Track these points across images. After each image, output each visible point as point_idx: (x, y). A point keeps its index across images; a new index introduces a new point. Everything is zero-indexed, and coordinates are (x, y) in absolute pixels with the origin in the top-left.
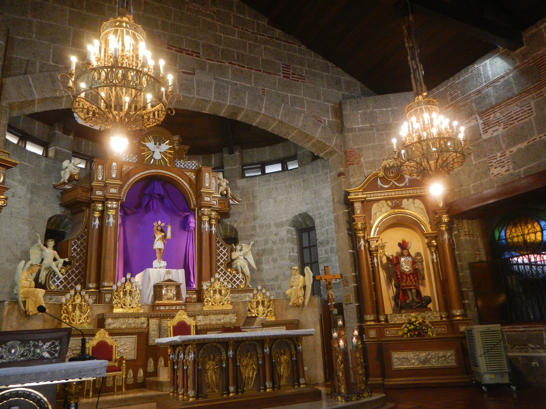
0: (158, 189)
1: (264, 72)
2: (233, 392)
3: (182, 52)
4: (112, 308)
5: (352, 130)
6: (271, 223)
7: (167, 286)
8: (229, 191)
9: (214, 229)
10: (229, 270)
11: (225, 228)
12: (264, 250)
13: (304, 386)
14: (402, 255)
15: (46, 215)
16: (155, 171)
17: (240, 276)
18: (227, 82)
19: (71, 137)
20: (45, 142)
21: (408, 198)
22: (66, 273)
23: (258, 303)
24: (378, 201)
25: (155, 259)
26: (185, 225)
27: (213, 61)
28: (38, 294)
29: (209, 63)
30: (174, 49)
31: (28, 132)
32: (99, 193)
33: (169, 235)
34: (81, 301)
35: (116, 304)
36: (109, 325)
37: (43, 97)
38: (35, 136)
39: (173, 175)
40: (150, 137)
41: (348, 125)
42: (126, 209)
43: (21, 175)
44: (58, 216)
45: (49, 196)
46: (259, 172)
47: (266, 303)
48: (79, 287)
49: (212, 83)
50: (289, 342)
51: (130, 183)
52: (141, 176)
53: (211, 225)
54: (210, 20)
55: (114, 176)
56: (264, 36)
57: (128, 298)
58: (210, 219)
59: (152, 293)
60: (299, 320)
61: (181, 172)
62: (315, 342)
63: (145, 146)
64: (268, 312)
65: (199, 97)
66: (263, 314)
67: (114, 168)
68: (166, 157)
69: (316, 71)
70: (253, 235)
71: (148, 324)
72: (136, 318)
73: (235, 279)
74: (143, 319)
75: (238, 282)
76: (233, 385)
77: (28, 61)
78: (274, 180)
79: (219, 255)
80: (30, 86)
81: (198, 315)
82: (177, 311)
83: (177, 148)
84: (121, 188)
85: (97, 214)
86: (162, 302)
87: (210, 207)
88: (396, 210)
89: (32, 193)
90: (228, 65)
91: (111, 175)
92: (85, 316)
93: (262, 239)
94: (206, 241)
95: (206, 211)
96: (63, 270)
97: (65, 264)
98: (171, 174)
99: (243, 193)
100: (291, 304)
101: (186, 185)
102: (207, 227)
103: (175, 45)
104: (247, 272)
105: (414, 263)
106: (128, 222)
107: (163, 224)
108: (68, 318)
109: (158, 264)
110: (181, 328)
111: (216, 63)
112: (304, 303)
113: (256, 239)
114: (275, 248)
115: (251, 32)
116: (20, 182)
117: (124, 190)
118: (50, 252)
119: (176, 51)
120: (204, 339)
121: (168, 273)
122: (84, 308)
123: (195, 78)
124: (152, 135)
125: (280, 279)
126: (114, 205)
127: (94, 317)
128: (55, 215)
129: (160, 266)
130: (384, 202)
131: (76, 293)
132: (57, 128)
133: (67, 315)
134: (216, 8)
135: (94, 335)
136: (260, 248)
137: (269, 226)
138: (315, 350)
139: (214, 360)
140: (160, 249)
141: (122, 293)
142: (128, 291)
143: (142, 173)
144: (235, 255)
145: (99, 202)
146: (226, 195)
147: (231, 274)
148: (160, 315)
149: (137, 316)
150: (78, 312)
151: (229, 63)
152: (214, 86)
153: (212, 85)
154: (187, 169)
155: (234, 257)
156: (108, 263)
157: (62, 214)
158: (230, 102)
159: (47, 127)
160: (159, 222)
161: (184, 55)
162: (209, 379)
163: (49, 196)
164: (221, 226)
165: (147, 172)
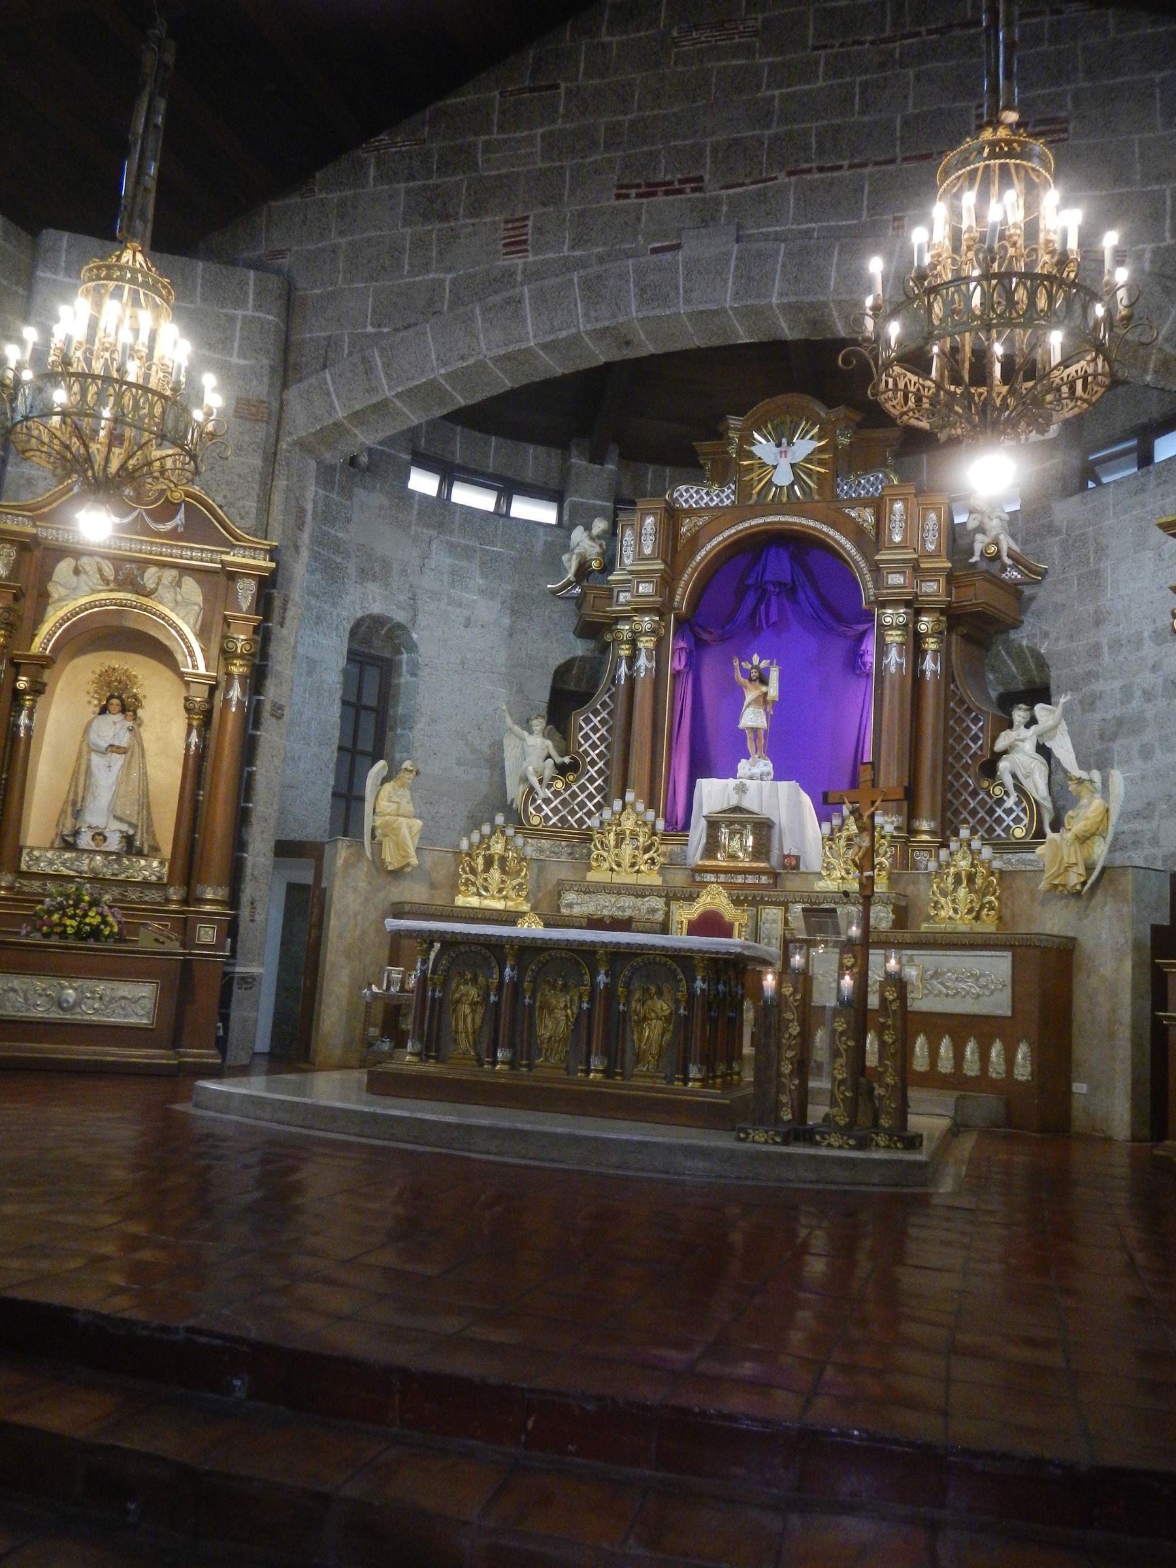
1: (905, 159)
2: (503, 1063)
3: (654, 194)
6: (1142, 632)
7: (730, 823)
10: (986, 784)
11: (1018, 654)
12: (1120, 722)
13: (698, 1084)
15: (550, 660)
16: (761, 521)
18: (778, 237)
19: (611, 467)
20: (555, 491)
22: (566, 790)
26: (854, 660)
27: (742, 185)
28: (399, 829)
29: (728, 196)
30: (633, 192)
31: (509, 474)
34: (506, 849)
35: (597, 860)
36: (570, 906)
37: (350, 412)
38: (529, 480)
39: (811, 523)
40: (766, 427)
42: (697, 629)
43: (484, 576)
44: (582, 658)
45: (555, 616)
46: (1128, 467)
47: (979, 881)
49: (728, 254)
50: (674, 966)
51: (699, 564)
52: (725, 539)
54: (744, 62)
55: (647, 551)
56: (917, 34)
59: (704, 841)
60: (1073, 940)
62: (1113, 1011)
63: (751, 456)
64: (982, 907)
65: (689, 309)
66: (970, 911)
67: (649, 530)
68: (809, 476)
69: (1119, 80)
70: (1091, 676)
71: (667, 914)
72: (637, 896)
73: (999, 812)
74: (658, 903)
75: (1008, 820)
76: (511, 1045)
77: (330, 337)
78: (1159, 485)
79: (959, 739)
80: (329, 394)
81: (796, 902)
82: (705, 884)
83: (846, 441)
86: (714, 863)
87: (908, 604)
89: (514, 612)
90: (787, 180)
91: (640, 551)
92: (515, 883)
93: (1117, 684)
94: (891, 702)
95: (890, 616)
96: (559, 785)
98: (804, 521)
99: (1071, 542)
100: (1043, 886)
101: (849, 546)
102: (893, 661)
103: (637, 181)
104: (1038, 786)
107: (764, 664)
108: (473, 884)
109: (748, 766)
110: (710, 924)
111: (751, 188)
112: (1084, 884)
113: (1098, 686)
114: (1150, 711)
115: (873, 43)
116: (482, 592)
117: (682, 583)
119: (639, 196)
120: (430, 931)
122: (512, 865)
123: (680, 256)
124: (772, 421)
125: (1157, 813)
127: (550, 887)
128: (573, 660)
129: (749, 773)
131: (493, 833)
132: (574, 451)
133: (471, 877)
134: (760, 17)
136: (1109, 716)
137: (1137, 642)
138: (1112, 1036)
139: (474, 980)
140: (755, 730)
142: (628, 832)
143: (726, 534)
146: (997, 556)
147: (991, 797)
148: (738, 897)
149: (639, 892)
150: (495, 874)
151: (790, 174)
152: (733, 263)
153: (729, 260)
154: (864, 498)
155: (1000, 745)
157: (589, 654)
158: (781, 295)
159: (555, 453)
160: (756, 658)
161: (660, 198)
162: (461, 1023)
163: (555, 616)
164: (1007, 653)
165: (740, 527)
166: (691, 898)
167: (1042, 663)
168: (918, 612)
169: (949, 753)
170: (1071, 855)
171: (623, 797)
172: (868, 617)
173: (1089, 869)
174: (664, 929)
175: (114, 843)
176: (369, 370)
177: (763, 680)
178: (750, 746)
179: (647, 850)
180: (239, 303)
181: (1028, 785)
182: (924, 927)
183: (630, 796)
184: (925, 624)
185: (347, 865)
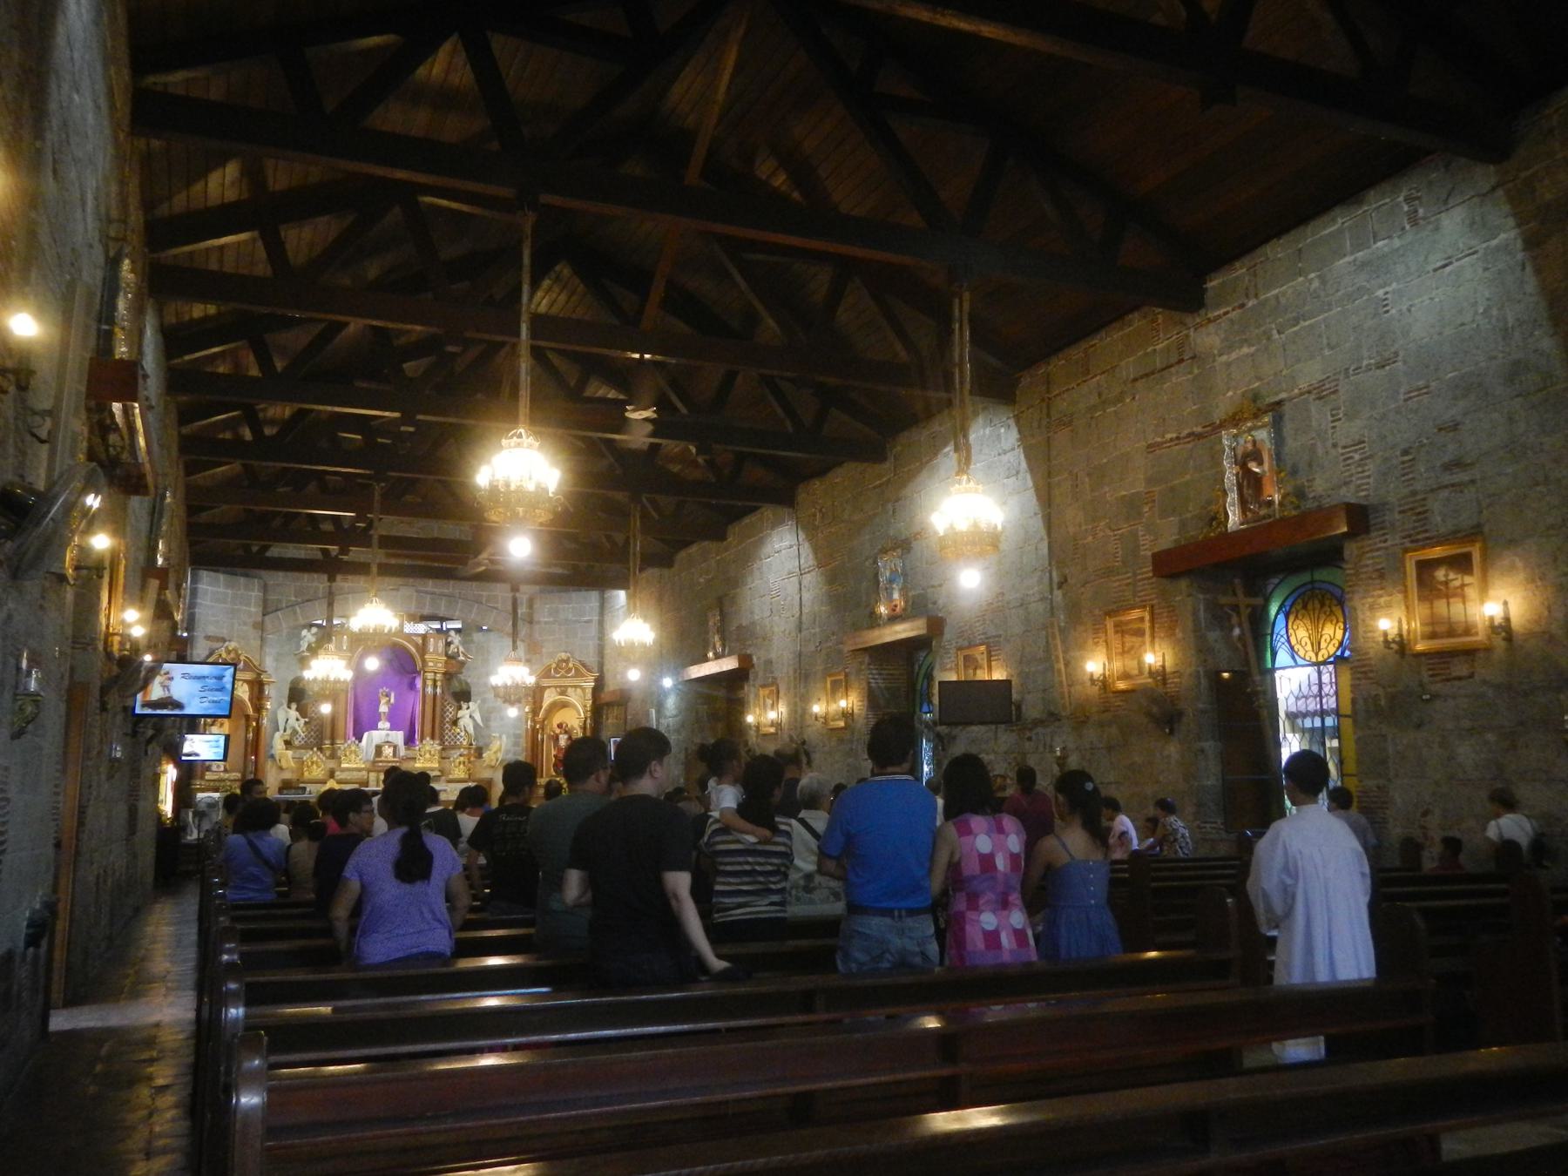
5: (539, 622)
8: (461, 649)
9: (439, 690)
11: (460, 682)
17: (463, 734)
18: (426, 593)
21: (571, 686)
23: (460, 763)
24: (549, 687)
25: (380, 720)
26: (412, 686)
33: (392, 700)
41: (536, 617)
48: (315, 749)
53: (435, 686)
58: (435, 681)
74: (364, 773)
95: (430, 676)
97: (306, 723)
104: (471, 729)
105: (570, 738)
118: (293, 713)
121: (388, 735)
130: (553, 689)
135: (325, 783)
144: (460, 713)
149: (359, 770)
150: (315, 767)
155: (459, 716)
167: (467, 684)
169: (443, 717)
170: (493, 757)
172: (419, 673)
175: (222, 769)
176: (295, 613)
177: (388, 695)
180: (253, 590)
181: (468, 729)
182: (451, 777)
184: (439, 677)
185: (272, 767)
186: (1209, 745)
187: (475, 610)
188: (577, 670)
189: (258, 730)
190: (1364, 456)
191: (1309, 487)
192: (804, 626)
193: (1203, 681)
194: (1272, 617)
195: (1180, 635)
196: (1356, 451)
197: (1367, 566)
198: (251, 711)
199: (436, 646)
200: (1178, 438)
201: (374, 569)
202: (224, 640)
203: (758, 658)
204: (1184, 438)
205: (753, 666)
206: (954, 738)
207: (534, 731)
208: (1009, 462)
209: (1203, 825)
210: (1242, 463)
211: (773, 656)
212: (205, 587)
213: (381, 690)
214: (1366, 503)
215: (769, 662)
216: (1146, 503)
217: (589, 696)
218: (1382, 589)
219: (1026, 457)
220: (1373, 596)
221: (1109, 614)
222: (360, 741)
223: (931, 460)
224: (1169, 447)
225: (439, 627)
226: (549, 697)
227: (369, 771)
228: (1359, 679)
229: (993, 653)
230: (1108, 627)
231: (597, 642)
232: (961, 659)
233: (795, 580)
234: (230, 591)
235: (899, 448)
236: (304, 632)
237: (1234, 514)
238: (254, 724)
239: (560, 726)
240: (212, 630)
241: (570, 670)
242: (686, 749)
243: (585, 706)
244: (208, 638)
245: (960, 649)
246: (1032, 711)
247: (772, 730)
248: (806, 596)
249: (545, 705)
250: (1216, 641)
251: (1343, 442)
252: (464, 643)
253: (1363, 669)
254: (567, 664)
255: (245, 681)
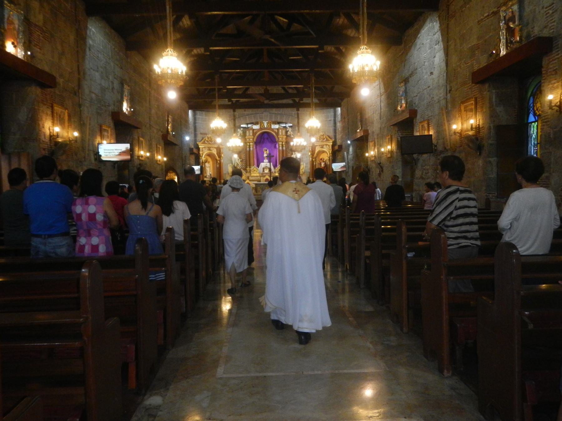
0: (266, 135)
4: (251, 174)
14: (322, 162)
18: (273, 113)
25: (264, 159)
26: (275, 147)
32: (248, 140)
53: (283, 147)
55: (251, 135)
57: (255, 172)
58: (282, 145)
61: (273, 130)
74: (259, 177)
84: (253, 139)
85: (248, 146)
88: (321, 149)
95: (280, 143)
96: (241, 163)
97: (241, 161)
105: (325, 164)
106: (258, 147)
107: (266, 149)
121: (266, 164)
126: (251, 144)
130: (319, 146)
141: (253, 171)
145: (248, 143)
146: (291, 134)
149: (257, 176)
156: (252, 161)
166: (264, 176)
168: (282, 142)
171: (254, 166)
172: (277, 142)
173: (302, 172)
174: (260, 181)
177: (266, 151)
178: (265, 158)
179: (257, 172)
183: (255, 166)
184: (284, 143)
186: (493, 160)
187: (290, 119)
188: (327, 139)
189: (220, 164)
190: (553, 11)
191: (532, 31)
192: (382, 117)
193: (492, 131)
194: (528, 98)
195: (484, 110)
196: (550, 9)
197: (551, 68)
198: (217, 158)
199: (282, 133)
200: (488, 15)
201: (217, 107)
202: (207, 134)
203: (371, 131)
204: (491, 15)
205: (369, 134)
206: (419, 159)
207: (312, 162)
208: (436, 38)
209: (488, 195)
210: (507, 24)
211: (374, 130)
212: (199, 116)
213: (264, 149)
214: (552, 36)
215: (373, 132)
216: (477, 49)
217: (331, 148)
218: (555, 79)
219: (441, 35)
220: (552, 84)
221: (463, 103)
222: (259, 167)
223: (414, 41)
224: (485, 20)
225: (285, 125)
226: (318, 149)
227: (261, 177)
228: (544, 125)
229: (430, 123)
230: (462, 108)
231: (333, 128)
232: (420, 126)
233: (379, 98)
234: (207, 117)
235: (406, 38)
236: (239, 130)
237: (503, 50)
238: (219, 162)
239: (321, 159)
240: (202, 131)
241: (324, 139)
242: (353, 167)
243: (329, 152)
244: (201, 134)
245: (421, 122)
246: (440, 148)
247: (373, 158)
248: (382, 104)
249: (316, 152)
250: (501, 112)
251: (545, 6)
252: (292, 131)
253: (545, 121)
254: (323, 137)
255: (214, 148)
